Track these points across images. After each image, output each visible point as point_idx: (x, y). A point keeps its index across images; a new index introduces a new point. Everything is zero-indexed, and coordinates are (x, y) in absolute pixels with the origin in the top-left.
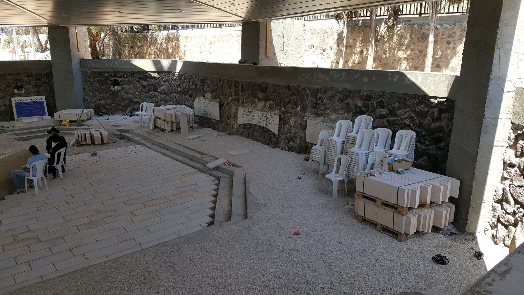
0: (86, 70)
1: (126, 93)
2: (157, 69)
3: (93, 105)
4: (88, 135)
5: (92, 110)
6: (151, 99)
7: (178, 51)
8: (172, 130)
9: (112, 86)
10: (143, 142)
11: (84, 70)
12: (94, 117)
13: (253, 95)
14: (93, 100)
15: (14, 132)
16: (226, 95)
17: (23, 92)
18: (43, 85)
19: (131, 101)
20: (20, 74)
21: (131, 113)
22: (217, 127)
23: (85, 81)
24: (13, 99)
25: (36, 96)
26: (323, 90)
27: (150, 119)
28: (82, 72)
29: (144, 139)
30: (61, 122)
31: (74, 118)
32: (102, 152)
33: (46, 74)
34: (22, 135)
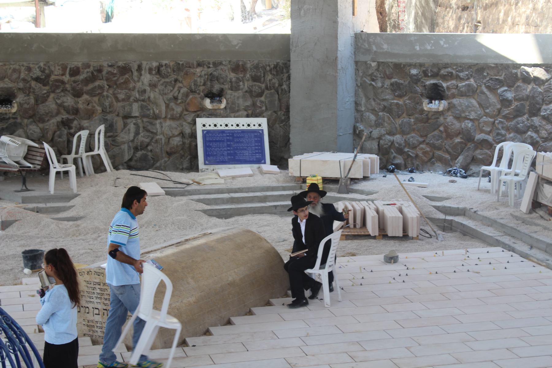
0: (367, 58)
1: (458, 118)
2: (544, 59)
3: (375, 145)
4: (371, 215)
5: (375, 157)
6: (520, 134)
9: (427, 101)
10: (506, 240)
11: (362, 58)
12: (378, 176)
14: (376, 133)
15: (202, 197)
17: (223, 106)
18: (266, 92)
19: (469, 138)
20: (221, 63)
21: (466, 168)
23: (361, 86)
24: (200, 122)
25: (248, 116)
27: (520, 186)
28: (356, 63)
29: (506, 234)
30: (304, 180)
31: (335, 174)
32: (408, 255)
33: (275, 67)
34: (217, 204)
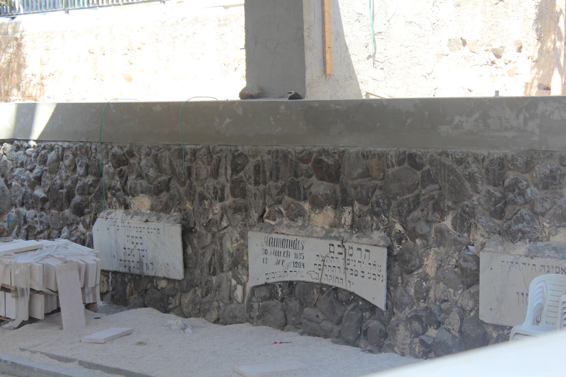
7: (20, 80)
8: (32, 320)
13: (295, 191)
16: (203, 198)
22: (174, 302)
26: (520, 161)
